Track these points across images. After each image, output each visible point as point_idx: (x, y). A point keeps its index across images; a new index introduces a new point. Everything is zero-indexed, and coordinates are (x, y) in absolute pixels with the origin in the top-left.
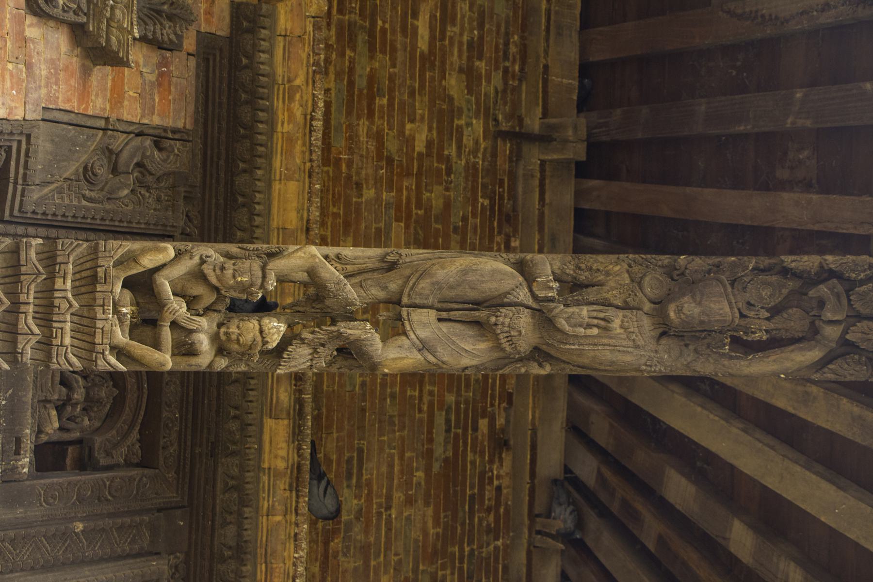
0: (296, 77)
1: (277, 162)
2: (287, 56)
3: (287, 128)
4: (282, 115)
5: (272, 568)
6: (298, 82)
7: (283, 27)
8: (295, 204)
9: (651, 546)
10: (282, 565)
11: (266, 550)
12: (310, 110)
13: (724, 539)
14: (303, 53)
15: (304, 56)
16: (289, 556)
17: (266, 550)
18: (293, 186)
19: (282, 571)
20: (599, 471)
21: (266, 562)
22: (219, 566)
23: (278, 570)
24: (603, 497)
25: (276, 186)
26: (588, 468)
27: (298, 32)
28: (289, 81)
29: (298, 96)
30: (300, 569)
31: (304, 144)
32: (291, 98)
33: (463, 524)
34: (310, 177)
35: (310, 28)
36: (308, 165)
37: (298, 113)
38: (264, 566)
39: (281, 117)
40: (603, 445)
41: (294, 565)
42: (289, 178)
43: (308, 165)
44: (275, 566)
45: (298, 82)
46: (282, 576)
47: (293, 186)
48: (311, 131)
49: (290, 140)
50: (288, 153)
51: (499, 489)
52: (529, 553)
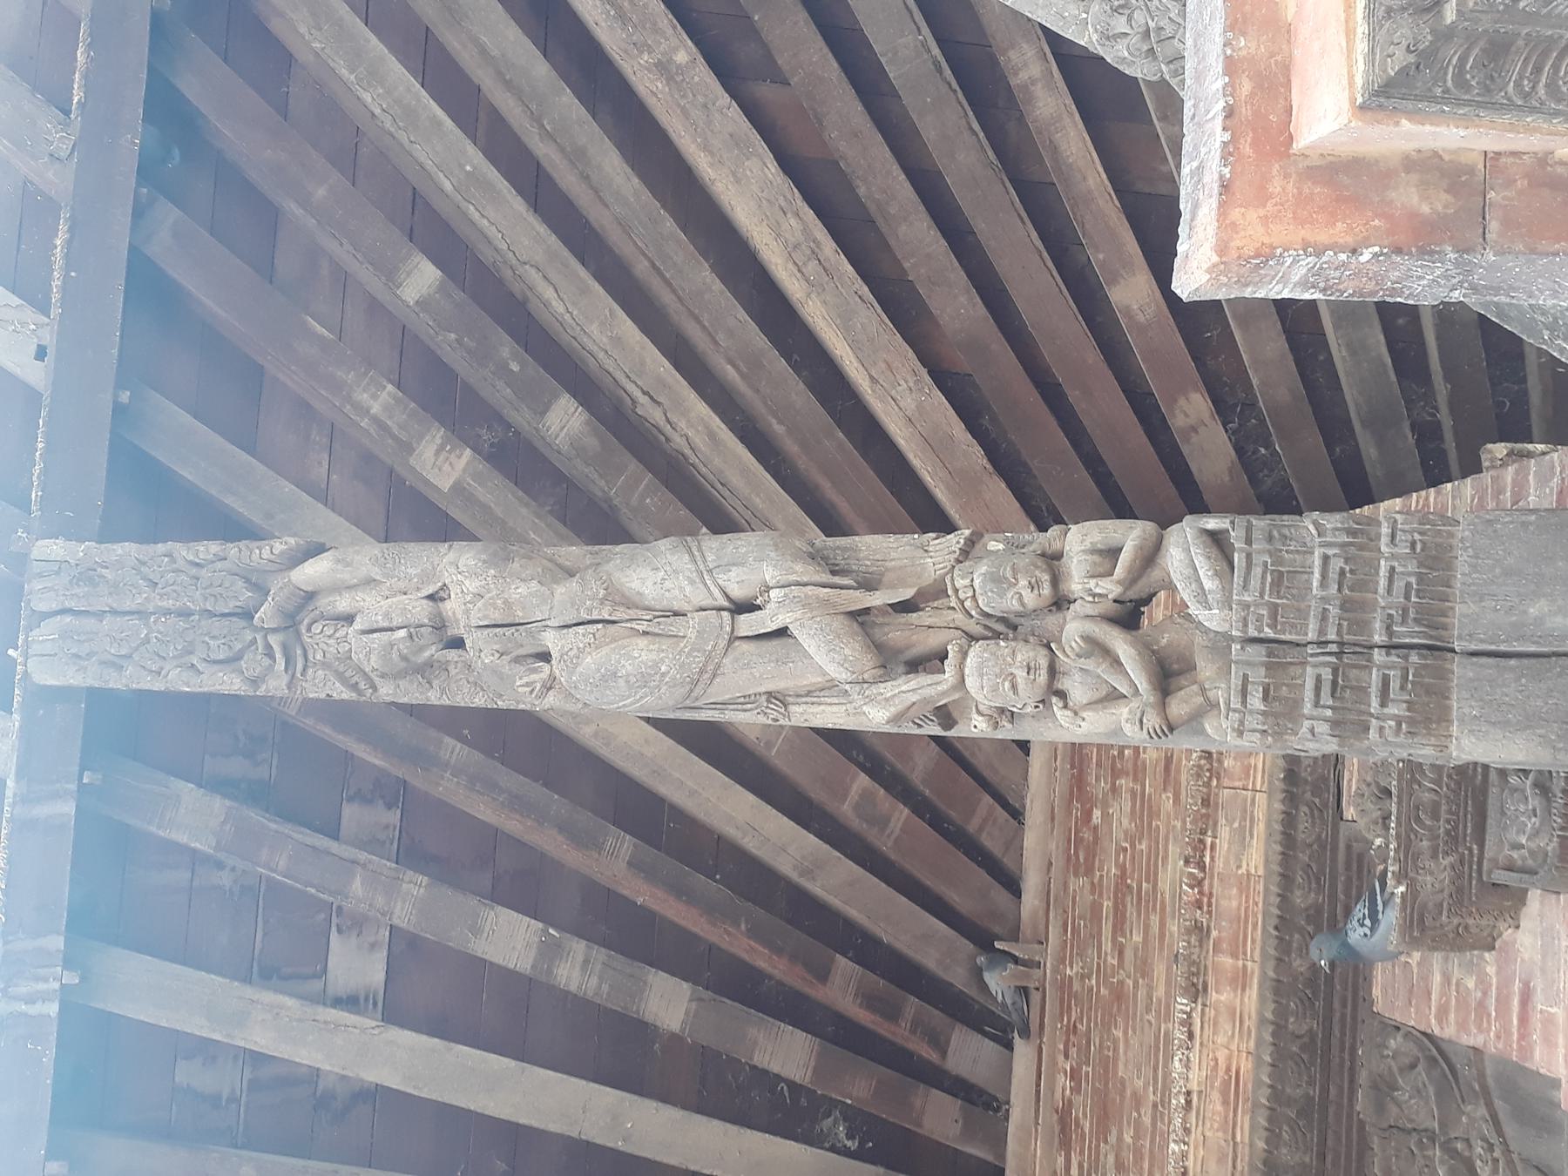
5: (1225, 1132)
9: (842, 962)
10: (1208, 1134)
11: (1234, 1167)
13: (700, 1000)
16: (1196, 1148)
17: (1234, 1167)
19: (1208, 1125)
20: (944, 1054)
21: (1235, 1144)
22: (1307, 1160)
23: (1216, 1126)
24: (936, 1016)
26: (968, 1053)
30: (1178, 1122)
33: (1096, 1024)
38: (1238, 1139)
40: (935, 1091)
41: (1187, 1131)
44: (1220, 1134)
46: (1208, 1115)
51: (1066, 1056)
52: (1047, 940)
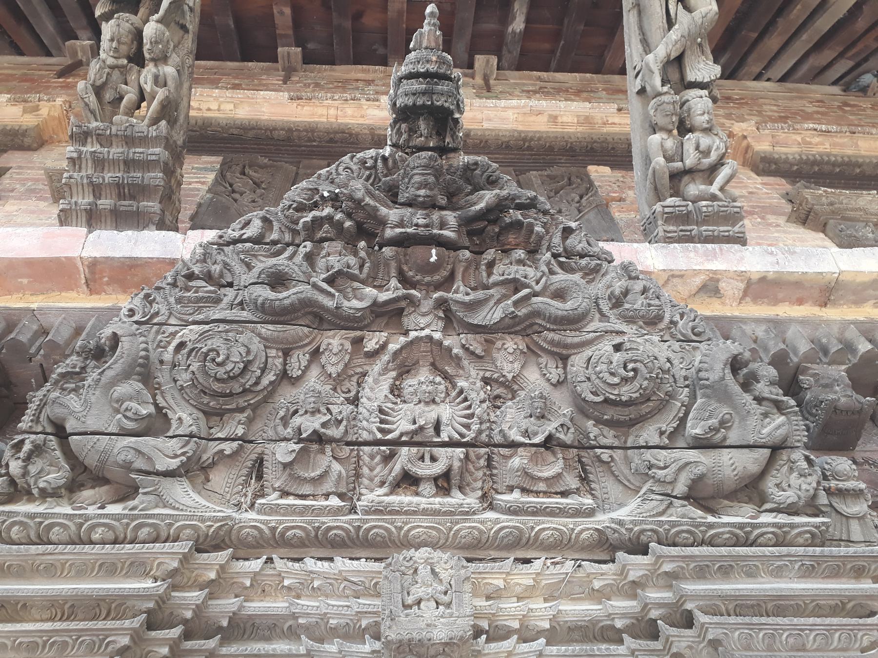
0: (796, 140)
1: (849, 152)
2: (786, 145)
3: (828, 146)
4: (821, 149)
6: (799, 139)
7: (768, 147)
8: (872, 142)
12: (815, 132)
14: (781, 135)
15: (784, 135)
18: (861, 143)
25: (863, 153)
27: (770, 139)
28: (799, 144)
29: (808, 139)
31: (836, 136)
32: (810, 143)
34: (854, 133)
35: (767, 132)
36: (848, 134)
37: (817, 140)
39: (821, 150)
42: (857, 146)
43: (848, 134)
45: (799, 139)
47: (861, 143)
48: (828, 132)
49: (834, 145)
50: (842, 145)
